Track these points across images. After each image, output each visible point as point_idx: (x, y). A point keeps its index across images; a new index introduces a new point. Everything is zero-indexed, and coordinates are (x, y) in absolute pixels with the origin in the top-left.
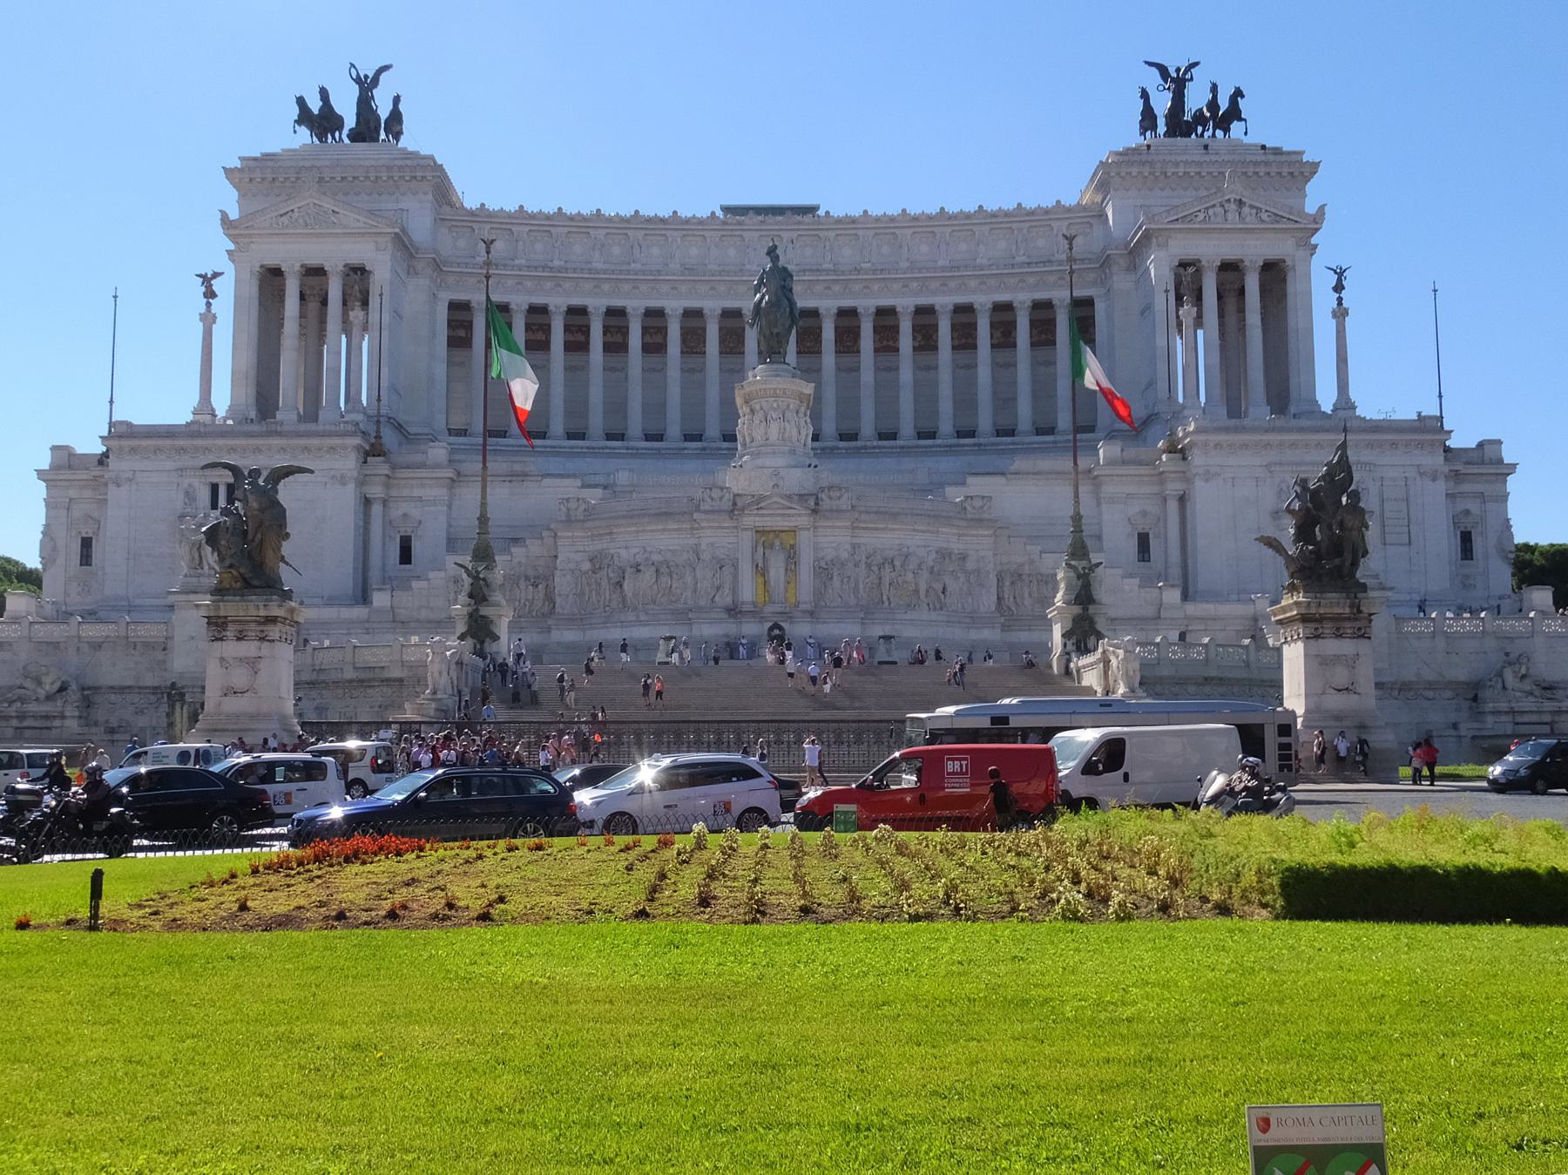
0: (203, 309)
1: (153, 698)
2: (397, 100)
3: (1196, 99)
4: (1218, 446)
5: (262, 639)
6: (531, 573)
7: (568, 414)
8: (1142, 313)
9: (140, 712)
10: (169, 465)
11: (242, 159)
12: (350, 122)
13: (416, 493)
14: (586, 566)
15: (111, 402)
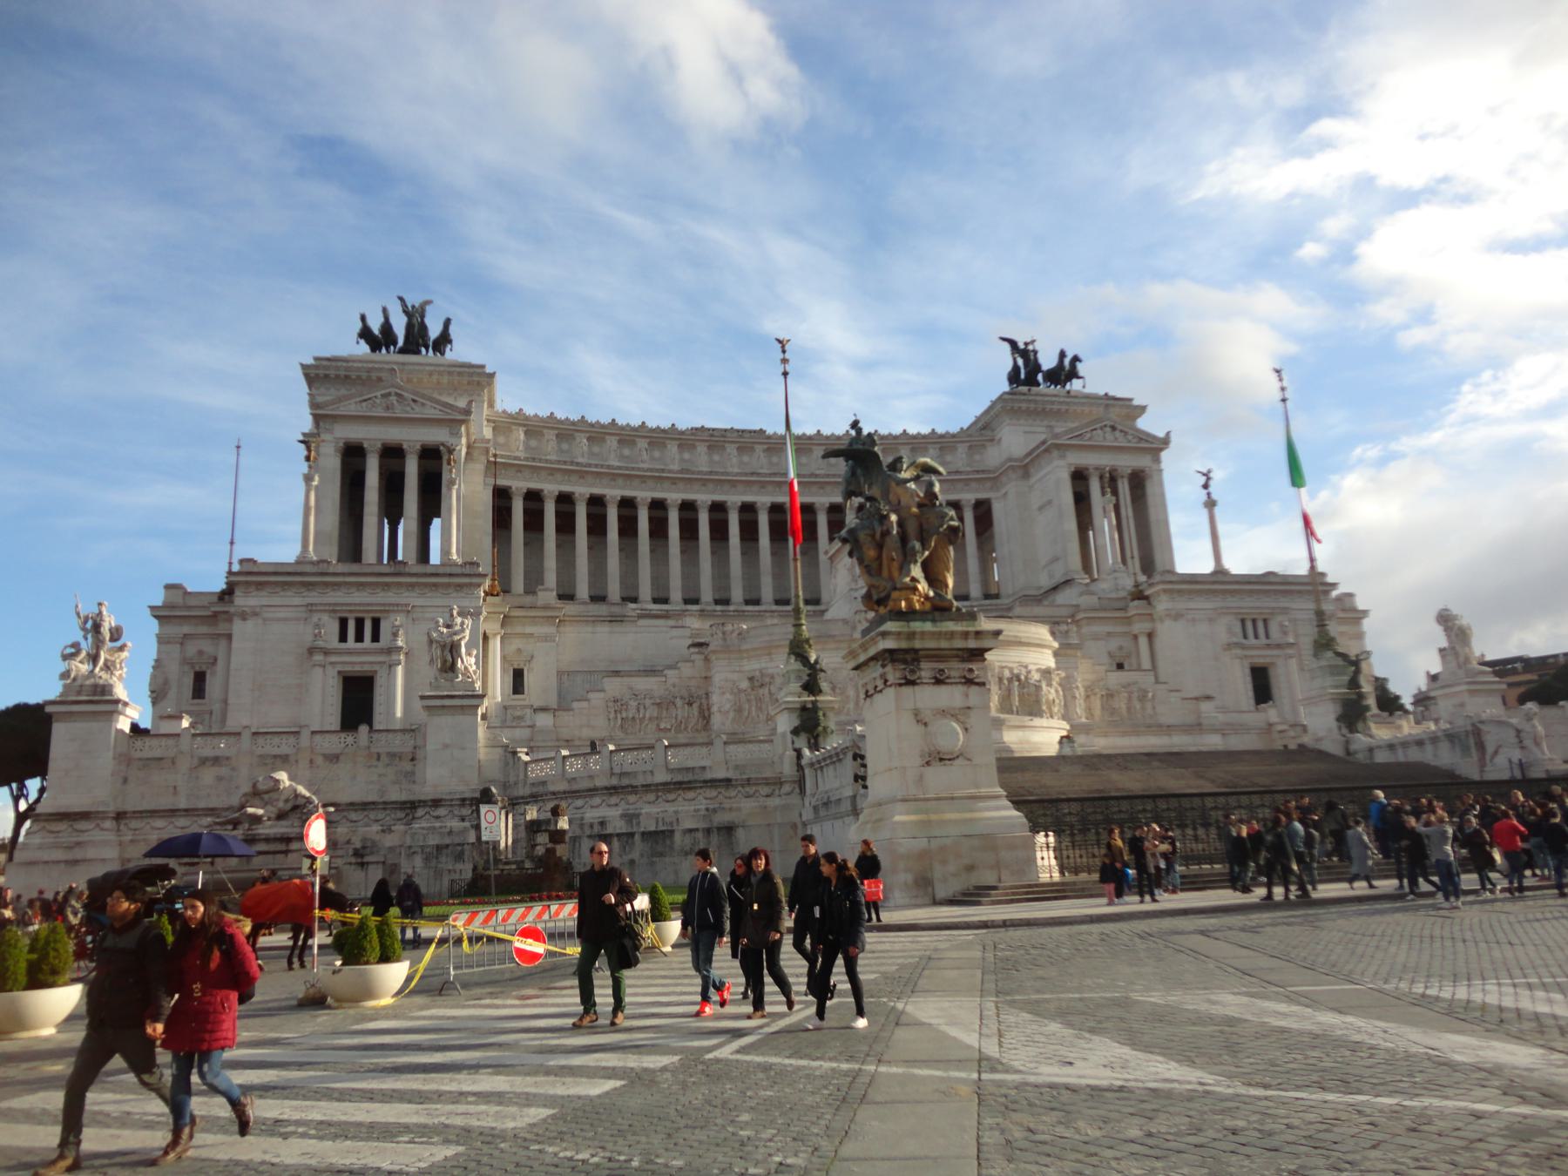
0: (304, 468)
1: (401, 814)
2: (447, 323)
3: (1048, 361)
4: (1179, 591)
5: (969, 682)
6: (686, 695)
7: (591, 585)
8: (1041, 508)
9: (387, 830)
10: (297, 601)
11: (316, 359)
12: (401, 342)
13: (529, 630)
14: (745, 684)
15: (232, 543)
